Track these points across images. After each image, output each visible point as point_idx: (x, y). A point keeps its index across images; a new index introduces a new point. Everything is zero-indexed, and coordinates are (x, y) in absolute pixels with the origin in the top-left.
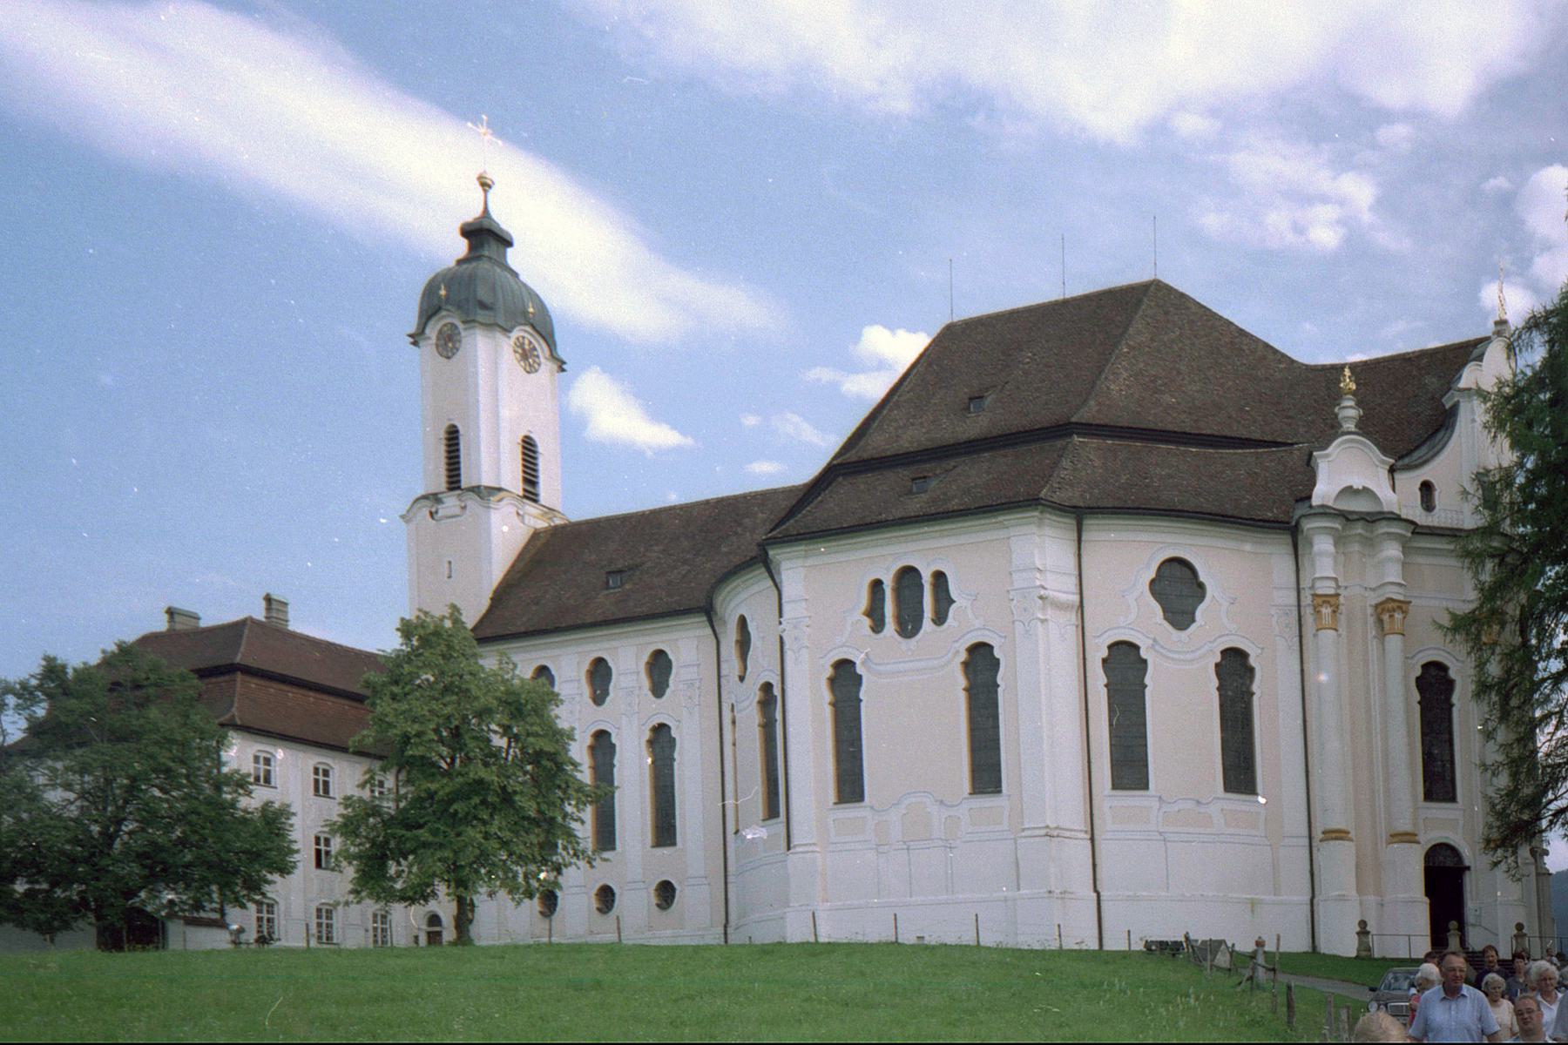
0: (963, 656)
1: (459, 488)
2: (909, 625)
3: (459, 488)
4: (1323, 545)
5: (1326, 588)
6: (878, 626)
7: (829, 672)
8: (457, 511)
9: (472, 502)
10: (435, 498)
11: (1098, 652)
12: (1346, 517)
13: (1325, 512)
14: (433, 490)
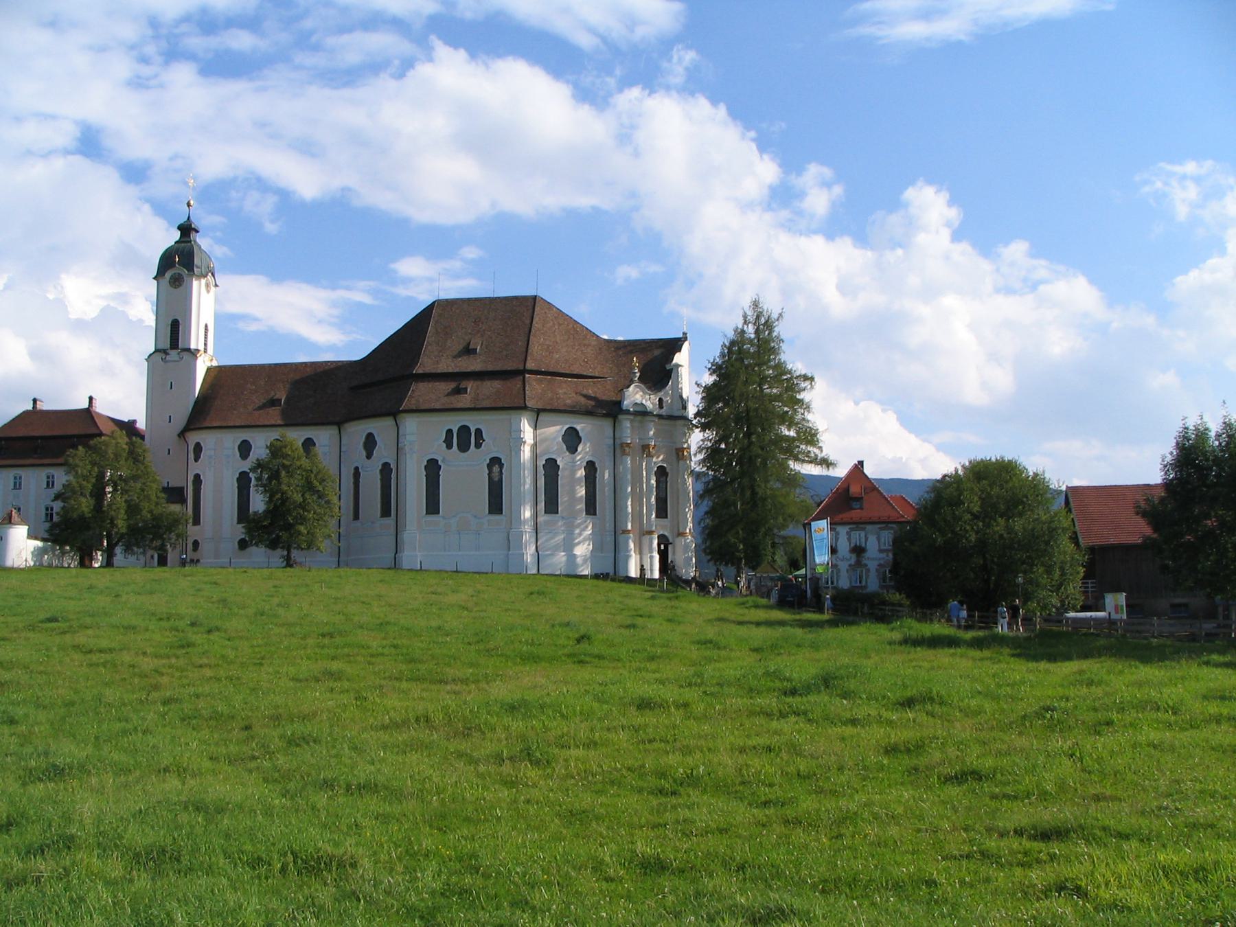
0: (488, 461)
1: (177, 348)
2: (463, 447)
3: (177, 348)
4: (626, 424)
5: (629, 442)
6: (449, 446)
7: (426, 463)
8: (178, 359)
9: (186, 355)
10: (165, 351)
11: (541, 462)
12: (636, 413)
13: (627, 412)
14: (160, 347)
